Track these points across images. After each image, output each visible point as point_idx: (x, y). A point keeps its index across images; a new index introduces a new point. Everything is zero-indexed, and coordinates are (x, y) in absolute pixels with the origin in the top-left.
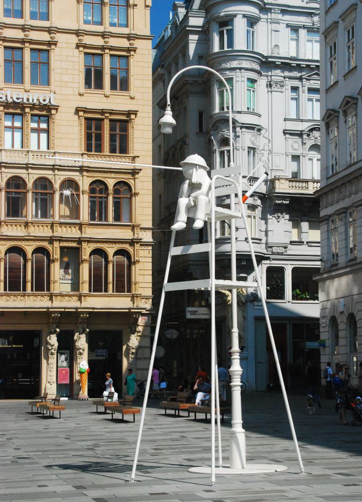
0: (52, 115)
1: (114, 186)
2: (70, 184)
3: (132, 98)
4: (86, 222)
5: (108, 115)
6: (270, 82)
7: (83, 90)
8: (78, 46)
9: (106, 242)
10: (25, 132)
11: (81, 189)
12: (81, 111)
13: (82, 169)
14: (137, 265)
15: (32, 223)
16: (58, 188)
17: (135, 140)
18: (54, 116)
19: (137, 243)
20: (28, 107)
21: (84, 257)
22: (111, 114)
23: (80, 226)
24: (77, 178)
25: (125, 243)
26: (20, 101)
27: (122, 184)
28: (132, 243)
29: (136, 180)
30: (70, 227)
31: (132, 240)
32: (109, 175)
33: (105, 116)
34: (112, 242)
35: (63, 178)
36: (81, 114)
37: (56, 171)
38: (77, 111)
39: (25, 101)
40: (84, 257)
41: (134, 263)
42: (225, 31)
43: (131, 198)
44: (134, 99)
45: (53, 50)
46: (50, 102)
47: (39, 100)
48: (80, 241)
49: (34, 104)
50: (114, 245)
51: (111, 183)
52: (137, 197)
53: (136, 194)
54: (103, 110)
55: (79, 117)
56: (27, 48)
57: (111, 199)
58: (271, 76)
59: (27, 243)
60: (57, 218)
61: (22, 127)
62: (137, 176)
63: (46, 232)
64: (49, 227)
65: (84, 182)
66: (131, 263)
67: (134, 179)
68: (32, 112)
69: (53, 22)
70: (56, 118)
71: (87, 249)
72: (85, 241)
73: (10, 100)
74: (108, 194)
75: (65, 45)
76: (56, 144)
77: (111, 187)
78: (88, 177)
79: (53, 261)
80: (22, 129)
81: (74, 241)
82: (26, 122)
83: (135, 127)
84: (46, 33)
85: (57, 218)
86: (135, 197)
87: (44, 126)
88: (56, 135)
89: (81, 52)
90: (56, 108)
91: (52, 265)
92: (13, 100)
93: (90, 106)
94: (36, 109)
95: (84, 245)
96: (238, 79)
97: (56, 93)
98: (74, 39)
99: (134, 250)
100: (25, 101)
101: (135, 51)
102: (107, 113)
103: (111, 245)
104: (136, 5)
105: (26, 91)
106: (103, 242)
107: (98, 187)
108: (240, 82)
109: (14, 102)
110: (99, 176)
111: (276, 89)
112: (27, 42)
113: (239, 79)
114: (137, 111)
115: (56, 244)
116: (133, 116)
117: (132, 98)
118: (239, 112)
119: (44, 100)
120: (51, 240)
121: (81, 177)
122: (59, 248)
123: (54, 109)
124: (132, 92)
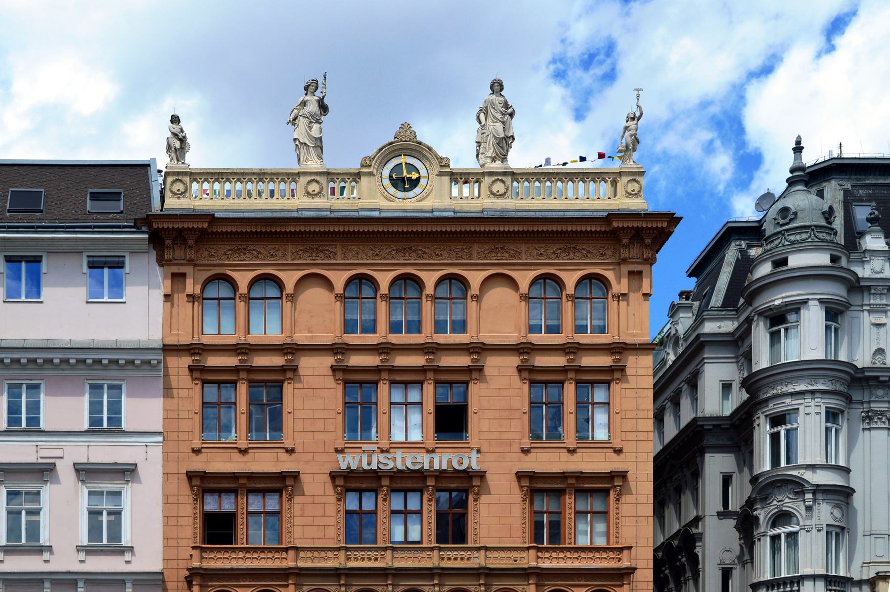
6: (868, 412)
7: (526, 443)
38: (520, 476)
42: (783, 331)
58: (869, 402)
73: (400, 467)
88: (483, 521)
93: (539, 468)
96: (808, 410)
97: (482, 450)
105: (429, 451)
108: (813, 414)
111: (880, 425)
113: (813, 410)
118: (813, 467)
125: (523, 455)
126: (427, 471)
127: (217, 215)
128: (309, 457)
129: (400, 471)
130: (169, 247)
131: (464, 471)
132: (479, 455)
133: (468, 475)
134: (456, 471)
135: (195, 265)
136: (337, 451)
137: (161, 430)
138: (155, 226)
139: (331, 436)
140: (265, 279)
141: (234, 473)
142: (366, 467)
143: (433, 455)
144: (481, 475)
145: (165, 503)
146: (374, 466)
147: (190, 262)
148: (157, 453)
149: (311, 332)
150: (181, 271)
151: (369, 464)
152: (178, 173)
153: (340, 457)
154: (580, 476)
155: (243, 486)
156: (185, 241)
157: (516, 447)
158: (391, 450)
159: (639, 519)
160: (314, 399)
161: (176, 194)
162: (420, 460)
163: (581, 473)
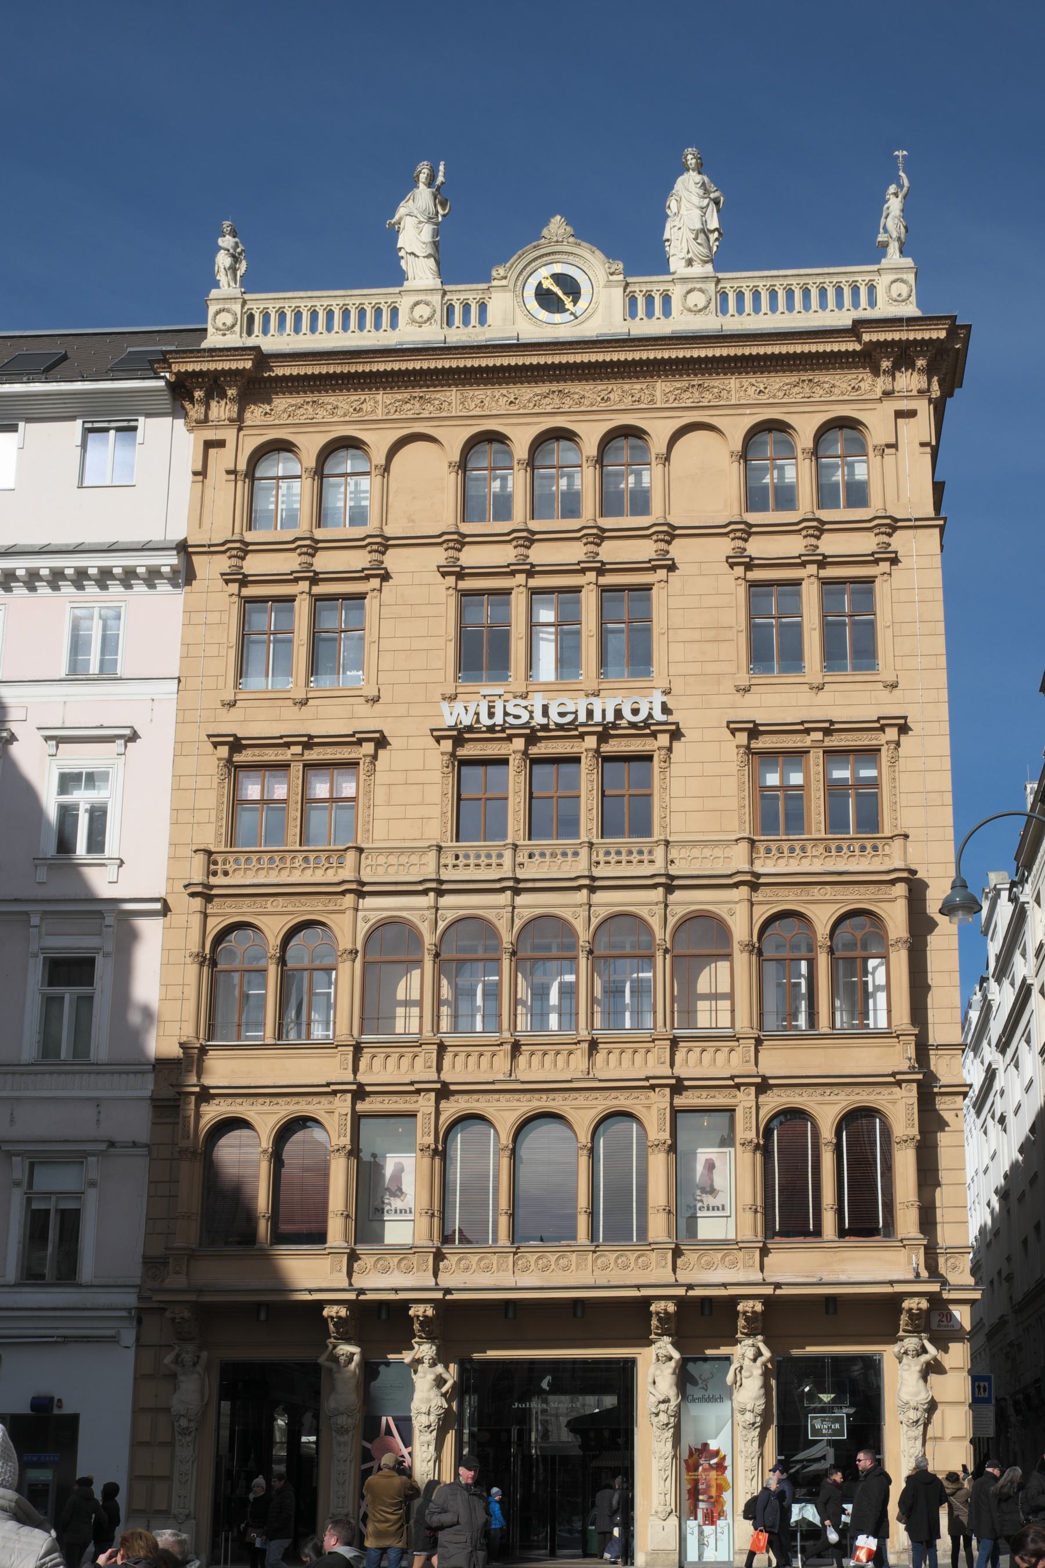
26: (569, 718)
32: (816, 892)
39: (582, 718)
119: (635, 712)
124: (886, 670)
125: (739, 695)
128: (402, 710)
132: (665, 699)
133: (646, 728)
142: (485, 720)
145: (176, 789)
146: (499, 719)
151: (491, 715)
157: (728, 686)
160: (412, 620)
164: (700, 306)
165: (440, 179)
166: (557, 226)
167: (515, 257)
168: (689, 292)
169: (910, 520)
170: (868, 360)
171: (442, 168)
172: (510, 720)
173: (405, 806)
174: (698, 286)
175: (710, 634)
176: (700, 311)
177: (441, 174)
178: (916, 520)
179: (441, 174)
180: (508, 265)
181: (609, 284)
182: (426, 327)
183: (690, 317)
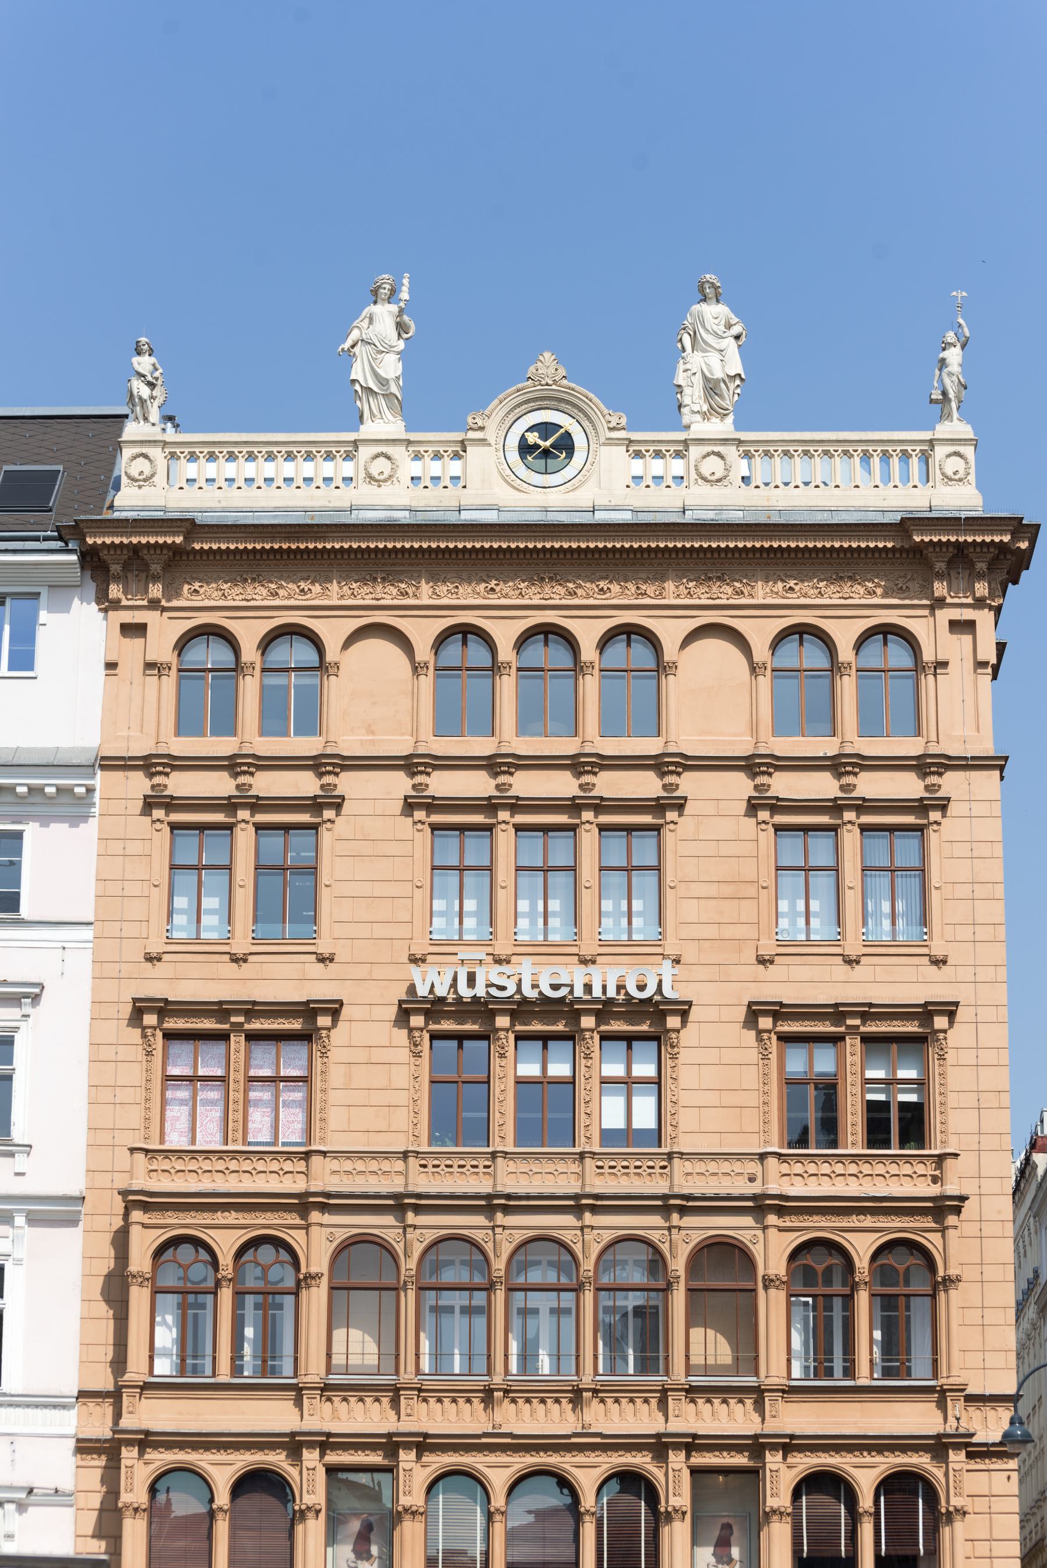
0: (668, 1031)
1: (874, 1257)
2: (723, 1256)
3: (939, 962)
4: (776, 1381)
5: (857, 1022)
8: (753, 807)
9: (850, 1449)
10: (581, 1095)
11: (761, 1272)
12: (765, 1013)
13: (760, 1206)
14: (958, 1525)
15: (595, 1391)
16: (682, 1272)
17: (952, 1099)
18: (674, 1035)
19: (957, 1447)
20: (588, 1012)
21: (772, 1502)
22: (866, 1017)
23: (758, 1394)
24: (745, 1236)
25: (916, 1449)
27: (903, 1250)
28: (939, 1446)
29: (951, 1233)
30: (724, 1401)
31: (938, 1437)
32: (854, 1221)
33: (848, 1027)
34: (870, 1449)
35: (697, 1237)
36: (765, 1022)
37: (675, 1216)
38: (754, 1012)
39: (579, 992)
40: (772, 1502)
41: (949, 1517)
43: (934, 1296)
44: (944, 962)
45: (672, 826)
46: (659, 990)
47: (624, 987)
48: (756, 1446)
49: (610, 1002)
50: (879, 1459)
51: (862, 1247)
52: (952, 1292)
53: (949, 1282)
54: (837, 1005)
55: (759, 1032)
56: (587, 826)
57: (862, 1298)
59: (580, 1458)
60: (679, 1375)
61: (574, 1076)
62: (951, 1220)
63: (641, 1420)
64: (654, 1402)
65: (772, 1249)
66: (939, 1518)
67: (943, 1231)
68: (603, 1028)
69: (672, 738)
70: (682, 1044)
71: (782, 1476)
72: (774, 1447)
74: (854, 1287)
75: (709, 808)
76: (682, 1127)
77: (862, 1263)
78: (781, 1230)
79: (669, 1517)
80: (574, 1083)
81: (739, 1449)
82: (583, 1061)
83: (951, 1057)
84: (651, 775)
85: (679, 1375)
86: (946, 1291)
87: (645, 1069)
88: (684, 1098)
89: (763, 826)
90: (684, 1010)
91: (665, 1531)
92: (540, 993)
93: (790, 995)
94: (618, 1016)
95: (773, 1460)
98: (741, 785)
99: (946, 1475)
100: (579, 992)
101: (943, 808)
102: (853, 1015)
103: (868, 1459)
104: (944, 664)
105: (584, 962)
106: (838, 1449)
107: (819, 1266)
109: (544, 999)
110: (821, 1226)
112: (588, 807)
114: (956, 1004)
115: (677, 1459)
116: (940, 1022)
117: (939, 962)
119: (641, 988)
120: (660, 1446)
121: (759, 1233)
122: (686, 1473)
123: (674, 1012)
126: (579, 1001)
127: (198, 522)
128: (362, 971)
129: (525, 1001)
130: (117, 579)
131: (650, 999)
134: (629, 998)
135: (164, 609)
136: (414, 960)
137: (91, 919)
138: (90, 541)
139: (404, 931)
140: (292, 634)
141: (221, 1003)
143: (591, 969)
144: (684, 1010)
146: (480, 991)
147: (154, 605)
148: (82, 963)
149: (373, 733)
150: (136, 621)
152: (142, 442)
153: (415, 973)
154: (868, 1012)
155: (237, 1027)
156: (145, 567)
158: (514, 959)
159: (982, 1096)
161: (137, 481)
162: (564, 979)
163: (871, 1005)
164: (717, 476)
165: (405, 295)
166: (547, 366)
167: (496, 402)
168: (704, 457)
169: (966, 758)
170: (918, 556)
171: (406, 281)
172: (494, 992)
173: (371, 1097)
174: (716, 449)
175: (728, 890)
176: (719, 480)
177: (405, 289)
178: (973, 758)
179: (405, 289)
180: (487, 412)
181: (610, 442)
182: (386, 488)
183: (705, 489)
